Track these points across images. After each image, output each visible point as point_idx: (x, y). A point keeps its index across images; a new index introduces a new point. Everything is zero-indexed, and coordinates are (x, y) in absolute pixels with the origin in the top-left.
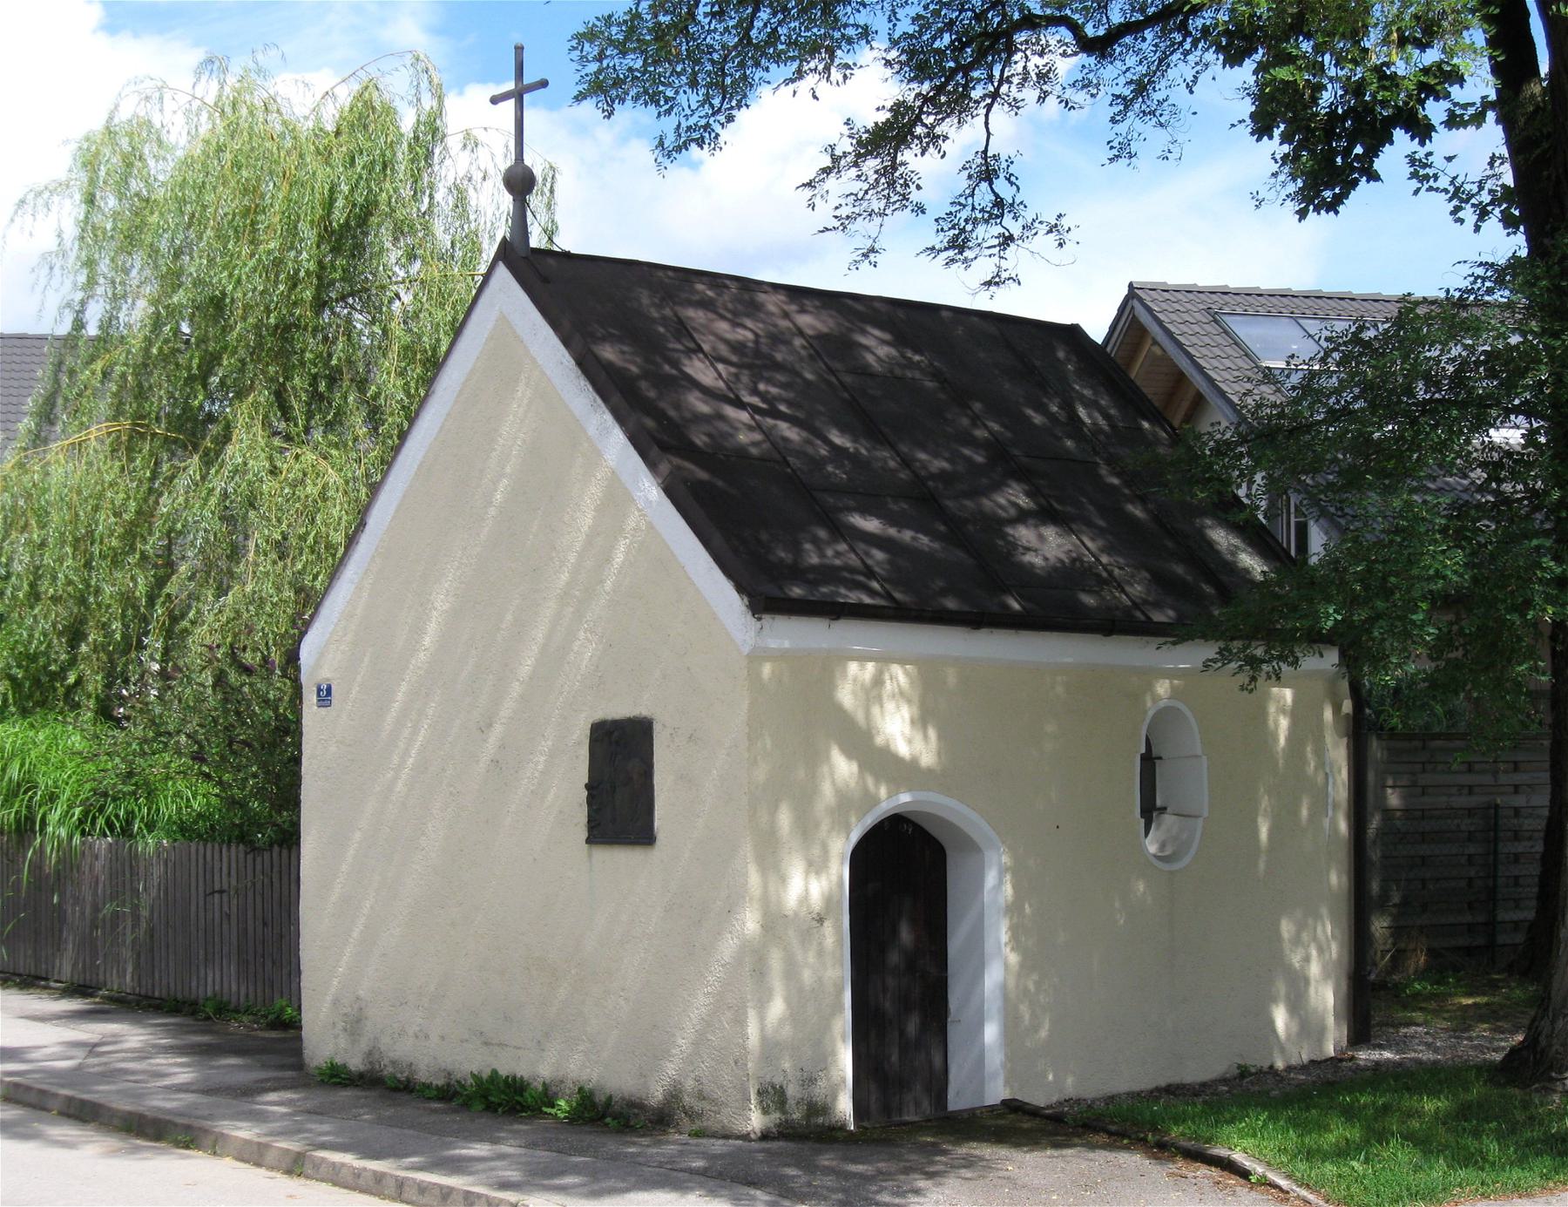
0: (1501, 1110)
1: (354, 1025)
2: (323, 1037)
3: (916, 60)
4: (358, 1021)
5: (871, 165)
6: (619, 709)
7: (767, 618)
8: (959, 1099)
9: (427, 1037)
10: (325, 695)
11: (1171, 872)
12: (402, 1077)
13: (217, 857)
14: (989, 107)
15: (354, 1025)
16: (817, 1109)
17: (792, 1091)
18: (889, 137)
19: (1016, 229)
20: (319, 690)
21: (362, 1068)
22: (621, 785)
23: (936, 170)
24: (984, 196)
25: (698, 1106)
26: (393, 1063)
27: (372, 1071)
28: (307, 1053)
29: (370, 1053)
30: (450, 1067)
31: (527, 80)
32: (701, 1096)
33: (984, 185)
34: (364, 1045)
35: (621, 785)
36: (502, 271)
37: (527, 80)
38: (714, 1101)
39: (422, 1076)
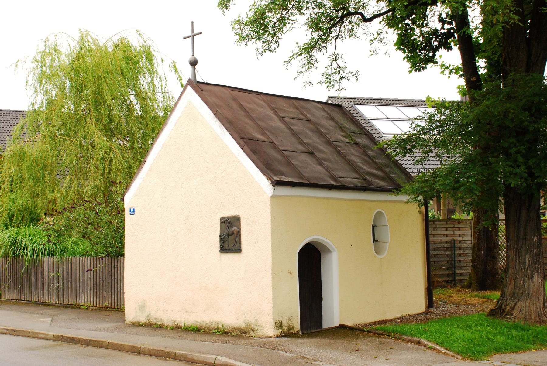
0: (511, 323)
1: (142, 307)
2: (132, 312)
3: (315, 24)
4: (144, 307)
5: (304, 56)
6: (229, 213)
7: (276, 187)
8: (326, 324)
9: (167, 311)
10: (132, 211)
11: (381, 259)
12: (160, 323)
13: (86, 261)
14: (337, 38)
15: (142, 307)
16: (291, 328)
17: (285, 323)
18: (309, 49)
19: (344, 75)
20: (130, 210)
21: (145, 321)
22: (230, 237)
23: (322, 57)
24: (335, 65)
25: (256, 328)
26: (156, 319)
27: (149, 322)
28: (126, 317)
29: (148, 316)
30: (174, 319)
31: (195, 32)
32: (257, 325)
33: (334, 62)
34: (146, 314)
35: (230, 237)
36: (189, 88)
37: (195, 32)
38: (261, 327)
39: (166, 323)
